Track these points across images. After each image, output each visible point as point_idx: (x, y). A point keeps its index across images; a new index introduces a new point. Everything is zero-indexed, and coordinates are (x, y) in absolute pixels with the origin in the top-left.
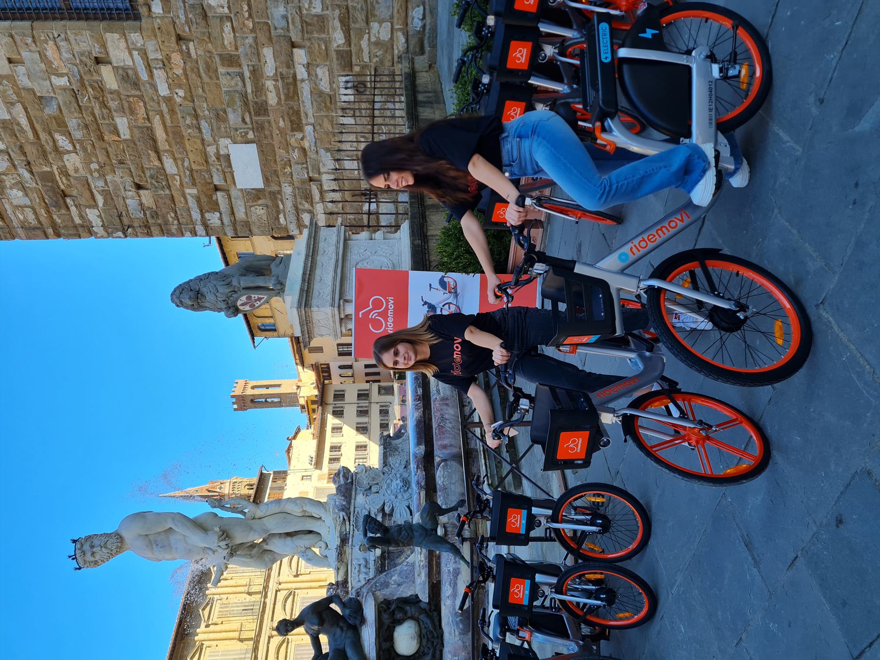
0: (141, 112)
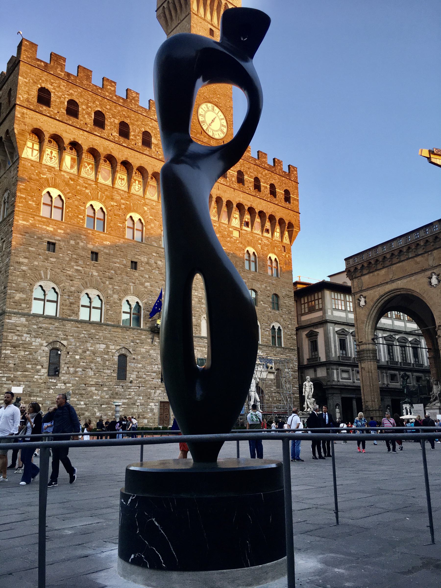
0: (32, 371)
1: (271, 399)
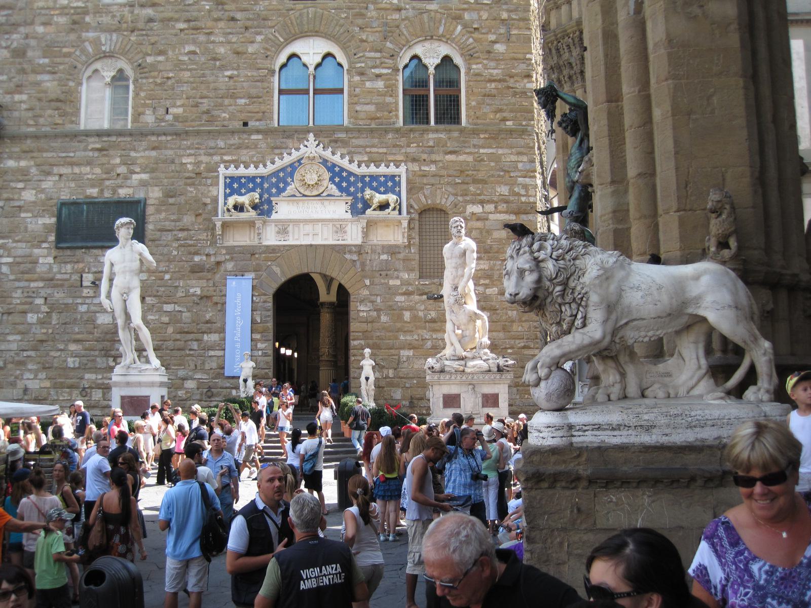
1: (384, 318)
